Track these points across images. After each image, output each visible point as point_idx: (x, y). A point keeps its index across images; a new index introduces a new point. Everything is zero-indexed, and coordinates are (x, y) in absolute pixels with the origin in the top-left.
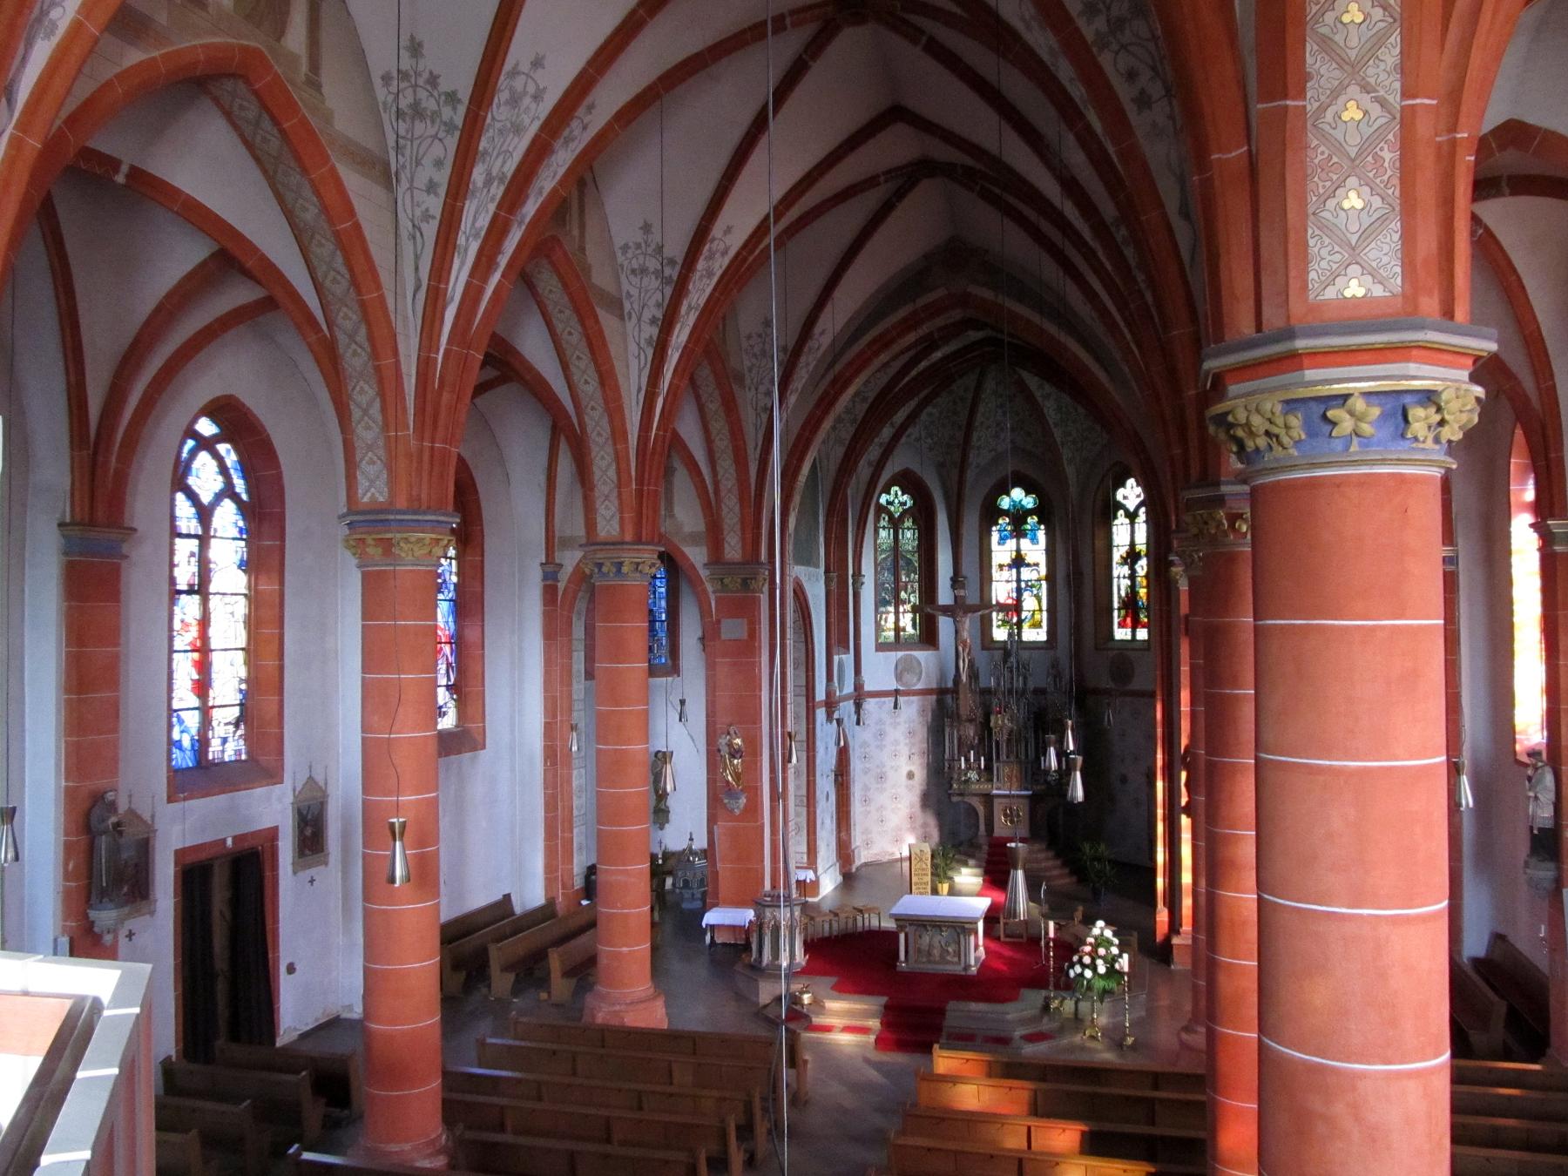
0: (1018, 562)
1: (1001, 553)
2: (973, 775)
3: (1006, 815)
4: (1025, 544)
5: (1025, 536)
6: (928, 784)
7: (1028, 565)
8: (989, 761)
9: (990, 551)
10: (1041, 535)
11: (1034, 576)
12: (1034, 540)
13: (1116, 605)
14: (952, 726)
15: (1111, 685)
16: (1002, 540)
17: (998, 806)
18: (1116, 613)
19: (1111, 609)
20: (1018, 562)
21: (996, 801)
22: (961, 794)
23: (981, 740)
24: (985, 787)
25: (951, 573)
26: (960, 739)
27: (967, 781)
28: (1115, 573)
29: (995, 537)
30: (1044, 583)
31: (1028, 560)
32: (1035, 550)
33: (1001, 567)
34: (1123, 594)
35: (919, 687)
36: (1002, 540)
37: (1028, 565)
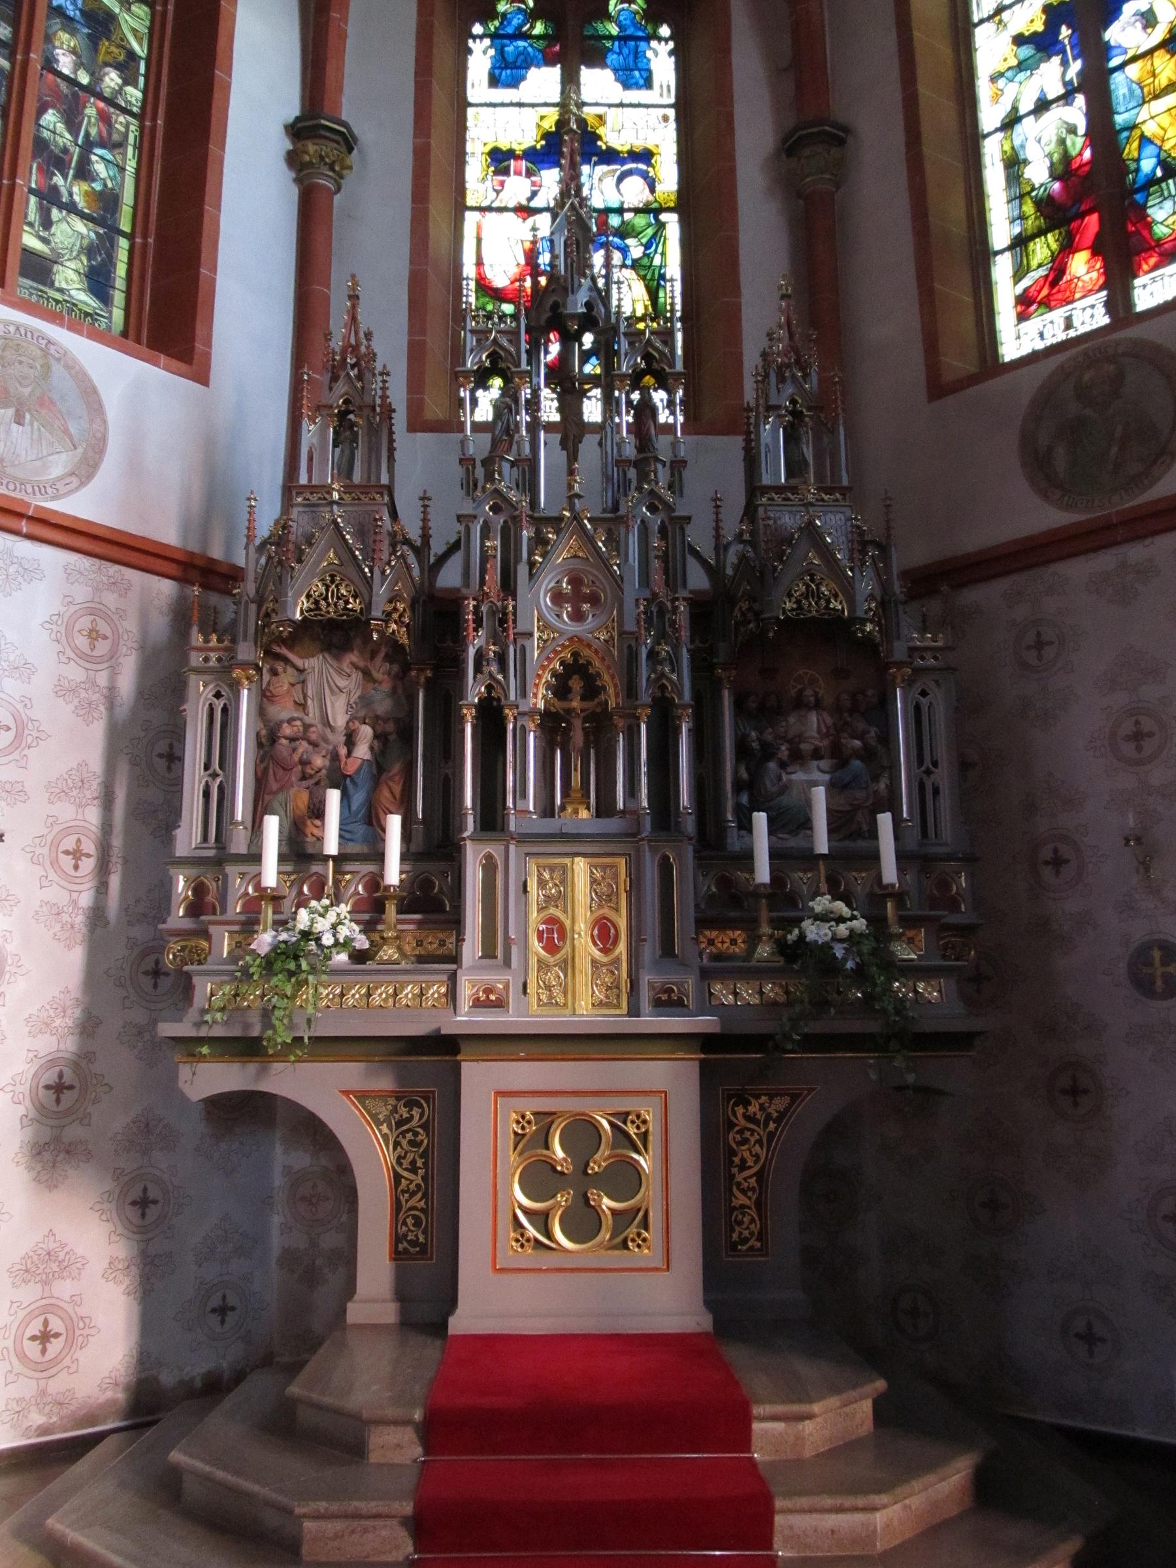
0: (570, 143)
1: (505, 113)
2: (332, 922)
3: (542, 1177)
4: (597, 84)
5: (596, 58)
6: (89, 1026)
7: (610, 156)
8: (436, 848)
9: (462, 104)
10: (662, 62)
11: (634, 192)
12: (634, 75)
13: (1001, 232)
14: (225, 675)
15: (1049, 517)
16: (506, 72)
17: (491, 1104)
18: (1002, 269)
19: (982, 256)
20: (570, 143)
21: (478, 1078)
22: (248, 1048)
23: (394, 739)
24: (407, 1002)
25: (292, 109)
26: (267, 742)
27: (292, 957)
28: (990, 116)
29: (480, 59)
30: (671, 220)
31: (613, 137)
32: (638, 112)
33: (500, 159)
34: (1038, 173)
35: (81, 506)
36: (506, 72)
37: (610, 156)
